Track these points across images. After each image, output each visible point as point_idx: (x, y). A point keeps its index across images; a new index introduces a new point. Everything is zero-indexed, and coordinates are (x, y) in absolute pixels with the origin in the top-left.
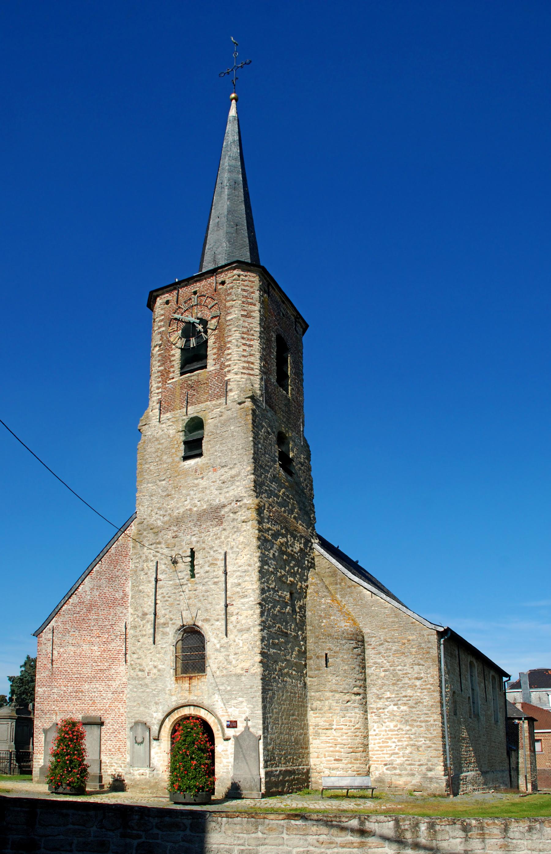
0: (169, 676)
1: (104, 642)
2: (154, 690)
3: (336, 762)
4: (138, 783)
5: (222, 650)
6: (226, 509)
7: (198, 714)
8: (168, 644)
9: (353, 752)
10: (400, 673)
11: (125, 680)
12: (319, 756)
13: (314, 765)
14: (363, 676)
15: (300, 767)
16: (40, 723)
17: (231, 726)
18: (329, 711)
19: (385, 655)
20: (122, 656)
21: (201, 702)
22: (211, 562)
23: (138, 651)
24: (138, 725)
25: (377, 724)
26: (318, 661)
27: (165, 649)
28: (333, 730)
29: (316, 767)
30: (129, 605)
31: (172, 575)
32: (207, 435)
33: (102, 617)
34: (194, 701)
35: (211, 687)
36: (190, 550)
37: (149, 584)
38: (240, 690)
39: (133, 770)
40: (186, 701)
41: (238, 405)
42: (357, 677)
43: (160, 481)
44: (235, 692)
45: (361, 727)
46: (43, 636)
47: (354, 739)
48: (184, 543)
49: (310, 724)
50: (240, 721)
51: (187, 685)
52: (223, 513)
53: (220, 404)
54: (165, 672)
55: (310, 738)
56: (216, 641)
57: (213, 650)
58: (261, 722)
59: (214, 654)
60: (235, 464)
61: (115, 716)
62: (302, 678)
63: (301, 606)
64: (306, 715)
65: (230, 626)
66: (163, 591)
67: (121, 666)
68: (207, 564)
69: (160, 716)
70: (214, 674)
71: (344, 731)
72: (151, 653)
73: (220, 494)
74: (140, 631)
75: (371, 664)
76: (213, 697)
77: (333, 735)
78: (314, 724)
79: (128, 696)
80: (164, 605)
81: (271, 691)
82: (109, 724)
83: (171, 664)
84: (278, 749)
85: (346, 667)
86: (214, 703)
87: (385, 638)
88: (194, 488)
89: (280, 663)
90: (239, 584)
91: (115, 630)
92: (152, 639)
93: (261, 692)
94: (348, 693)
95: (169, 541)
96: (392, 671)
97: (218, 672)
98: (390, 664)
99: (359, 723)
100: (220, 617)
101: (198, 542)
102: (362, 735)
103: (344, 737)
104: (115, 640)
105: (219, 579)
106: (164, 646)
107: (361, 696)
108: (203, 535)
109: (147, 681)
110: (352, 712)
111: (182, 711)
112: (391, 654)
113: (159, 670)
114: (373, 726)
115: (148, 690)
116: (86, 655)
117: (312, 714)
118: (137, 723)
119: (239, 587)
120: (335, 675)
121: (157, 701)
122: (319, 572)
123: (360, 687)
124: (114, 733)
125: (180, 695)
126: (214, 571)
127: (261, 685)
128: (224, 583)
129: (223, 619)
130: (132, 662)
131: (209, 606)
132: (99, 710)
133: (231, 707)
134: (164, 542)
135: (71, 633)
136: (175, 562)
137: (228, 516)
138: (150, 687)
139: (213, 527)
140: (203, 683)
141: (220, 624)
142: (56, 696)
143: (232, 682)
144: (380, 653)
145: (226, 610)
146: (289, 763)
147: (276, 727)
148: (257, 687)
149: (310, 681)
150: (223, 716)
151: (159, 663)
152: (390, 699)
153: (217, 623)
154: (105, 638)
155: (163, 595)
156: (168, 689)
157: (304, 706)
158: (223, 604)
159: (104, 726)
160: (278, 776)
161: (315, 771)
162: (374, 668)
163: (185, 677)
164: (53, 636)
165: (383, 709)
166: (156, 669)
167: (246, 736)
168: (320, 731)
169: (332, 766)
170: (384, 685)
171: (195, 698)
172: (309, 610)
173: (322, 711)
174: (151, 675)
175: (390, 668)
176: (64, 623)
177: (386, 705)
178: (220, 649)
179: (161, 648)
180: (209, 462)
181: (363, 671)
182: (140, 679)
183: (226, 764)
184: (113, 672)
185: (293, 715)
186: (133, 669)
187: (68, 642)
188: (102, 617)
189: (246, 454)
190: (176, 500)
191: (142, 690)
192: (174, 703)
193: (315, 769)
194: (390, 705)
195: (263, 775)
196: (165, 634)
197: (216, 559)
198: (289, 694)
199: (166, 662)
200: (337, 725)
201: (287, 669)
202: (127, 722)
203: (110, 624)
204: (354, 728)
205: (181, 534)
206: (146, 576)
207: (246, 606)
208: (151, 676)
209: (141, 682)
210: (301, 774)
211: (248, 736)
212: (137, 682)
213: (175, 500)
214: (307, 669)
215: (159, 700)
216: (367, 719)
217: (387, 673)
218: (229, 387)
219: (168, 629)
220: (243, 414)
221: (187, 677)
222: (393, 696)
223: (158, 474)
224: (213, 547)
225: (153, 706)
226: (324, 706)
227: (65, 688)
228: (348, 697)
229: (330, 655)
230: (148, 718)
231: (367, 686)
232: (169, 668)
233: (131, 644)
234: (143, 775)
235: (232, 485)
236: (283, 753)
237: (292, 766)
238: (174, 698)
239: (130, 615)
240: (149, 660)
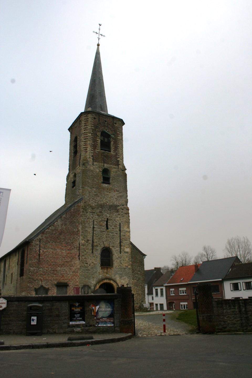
5: (119, 258)
6: (119, 207)
7: (110, 282)
10: (134, 269)
22: (115, 225)
30: (80, 235)
36: (106, 219)
40: (105, 277)
46: (34, 242)
48: (104, 215)
51: (106, 271)
56: (117, 255)
68: (113, 226)
69: (94, 282)
74: (86, 247)
79: (80, 274)
101: (110, 216)
115: (89, 272)
125: (103, 274)
126: (116, 229)
129: (119, 247)
130: (82, 260)
135: (50, 243)
137: (120, 210)
153: (117, 248)
158: (119, 241)
164: (40, 243)
171: (109, 276)
176: (46, 238)
187: (49, 247)
192: (101, 278)
196: (97, 250)
206: (89, 225)
212: (84, 268)
215: (94, 276)
219: (98, 248)
227: (47, 269)
232: (98, 263)
239: (81, 240)
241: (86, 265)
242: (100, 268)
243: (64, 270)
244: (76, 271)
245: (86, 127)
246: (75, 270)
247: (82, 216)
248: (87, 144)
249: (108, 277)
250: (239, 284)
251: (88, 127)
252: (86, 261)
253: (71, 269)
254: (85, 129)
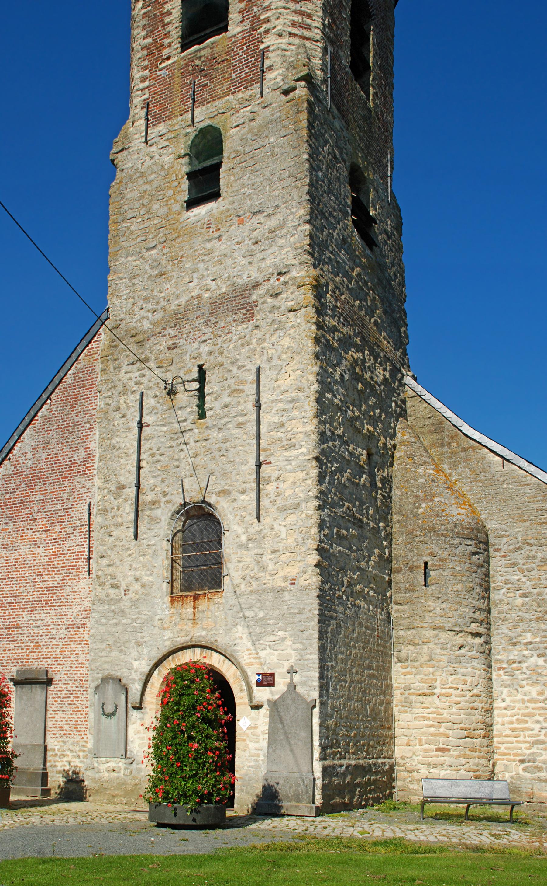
0: (159, 595)
1: (54, 539)
2: (135, 620)
3: (439, 753)
4: (105, 785)
7: (207, 661)
8: (159, 539)
9: (468, 737)
11: (87, 604)
12: (411, 743)
13: (401, 757)
14: (486, 604)
15: (380, 761)
17: (264, 682)
18: (429, 663)
19: (525, 567)
20: (82, 563)
21: (213, 640)
23: (109, 552)
24: (108, 683)
25: (508, 689)
26: (411, 575)
27: (154, 547)
28: (435, 697)
29: (404, 762)
31: (166, 416)
32: (228, 157)
33: (51, 496)
34: (201, 639)
35: (230, 613)
37: (128, 434)
38: (280, 616)
39: (97, 762)
40: (188, 638)
41: (283, 97)
42: (477, 604)
43: (148, 249)
44: (271, 621)
45: (482, 693)
47: (470, 714)
49: (395, 685)
50: (279, 674)
51: (191, 610)
52: (254, 297)
53: (251, 98)
54: (154, 587)
55: (396, 709)
57: (235, 545)
58: (317, 675)
59: (237, 553)
60: (277, 207)
61: (71, 667)
62: (385, 604)
63: (385, 478)
64: (389, 669)
65: (264, 502)
66: (152, 445)
67: (81, 580)
70: (236, 589)
71: (453, 698)
72: (130, 555)
73: (250, 263)
74: (113, 517)
75: (499, 584)
76: (234, 630)
77: (434, 705)
78: (403, 686)
80: (153, 469)
81: (334, 621)
82: (60, 682)
83: (163, 574)
84: (344, 727)
85: (459, 587)
86: (236, 642)
87: (525, 537)
88: (205, 257)
89: (349, 572)
90: (282, 425)
91: (71, 518)
92: (132, 530)
93: (316, 620)
94: (461, 631)
95: (161, 356)
96: (535, 596)
97: (243, 586)
98: (533, 583)
99: (479, 686)
100: (248, 486)
102: (482, 708)
103: (454, 710)
104: (72, 535)
105: (246, 417)
106: (153, 542)
107: (482, 638)
108: (220, 340)
109: (125, 604)
110: (468, 665)
111: (180, 657)
112: (534, 565)
113: (143, 586)
114: (502, 693)
116: (26, 563)
117: (400, 669)
118: (105, 680)
119: (282, 430)
120: (440, 600)
121: (139, 639)
122: (412, 425)
123: (481, 622)
124: (69, 697)
125: (177, 628)
127: (317, 607)
128: (255, 423)
130: (100, 573)
131: (229, 467)
132: (44, 658)
133: (265, 649)
134: (153, 358)
136: (172, 392)
138: (128, 616)
139: (237, 325)
140: (217, 606)
141: (248, 498)
143: (268, 604)
144: (515, 565)
145: (258, 473)
146: (362, 753)
147: (341, 686)
148: (310, 611)
149: (397, 611)
150: (251, 664)
151: (143, 573)
152: (532, 646)
154: (56, 532)
155: (151, 452)
156: (157, 617)
157: (386, 654)
159: (53, 686)
160: (344, 774)
161: (404, 768)
162: (504, 590)
163: (187, 596)
165: (520, 662)
166: (139, 584)
167: (289, 702)
168: (413, 698)
169: (432, 760)
170: (521, 620)
171: (204, 633)
172: (397, 488)
173: (417, 663)
174: (131, 595)
175: (532, 590)
177: (524, 656)
178: (247, 545)
179: (148, 545)
180: (231, 207)
181: (487, 595)
182: (112, 603)
183: (253, 752)
184: (68, 591)
185: (369, 668)
186: (100, 585)
188: (51, 496)
189: (296, 187)
190: (175, 282)
191: (115, 621)
192: (168, 643)
193: (404, 766)
194: (532, 656)
195: (318, 774)
197: (242, 382)
198: (364, 629)
199: (155, 570)
200: (442, 688)
201: (361, 586)
202: (90, 679)
203: (65, 507)
204: (471, 694)
205: (182, 342)
207: (294, 463)
208: (130, 596)
209: (113, 607)
210: (381, 773)
211: (294, 701)
212: (107, 607)
213: (173, 281)
214: (393, 590)
216: (491, 680)
217: (527, 599)
218: (267, 63)
220: (291, 112)
221: (191, 596)
222: (538, 640)
223: (144, 238)
224: (237, 360)
225: (134, 648)
226: (420, 654)
228: (461, 639)
229: (433, 565)
230: (125, 670)
231: (492, 623)
232: (160, 581)
233: (97, 540)
234: (114, 771)
235: (272, 246)
236: (352, 735)
237: (365, 758)
238: (168, 634)
240: (127, 567)
241: (112, 591)
243: (39, 623)
244: (78, 622)
246: (75, 618)
249: (201, 636)
252: (113, 577)
253: (61, 616)
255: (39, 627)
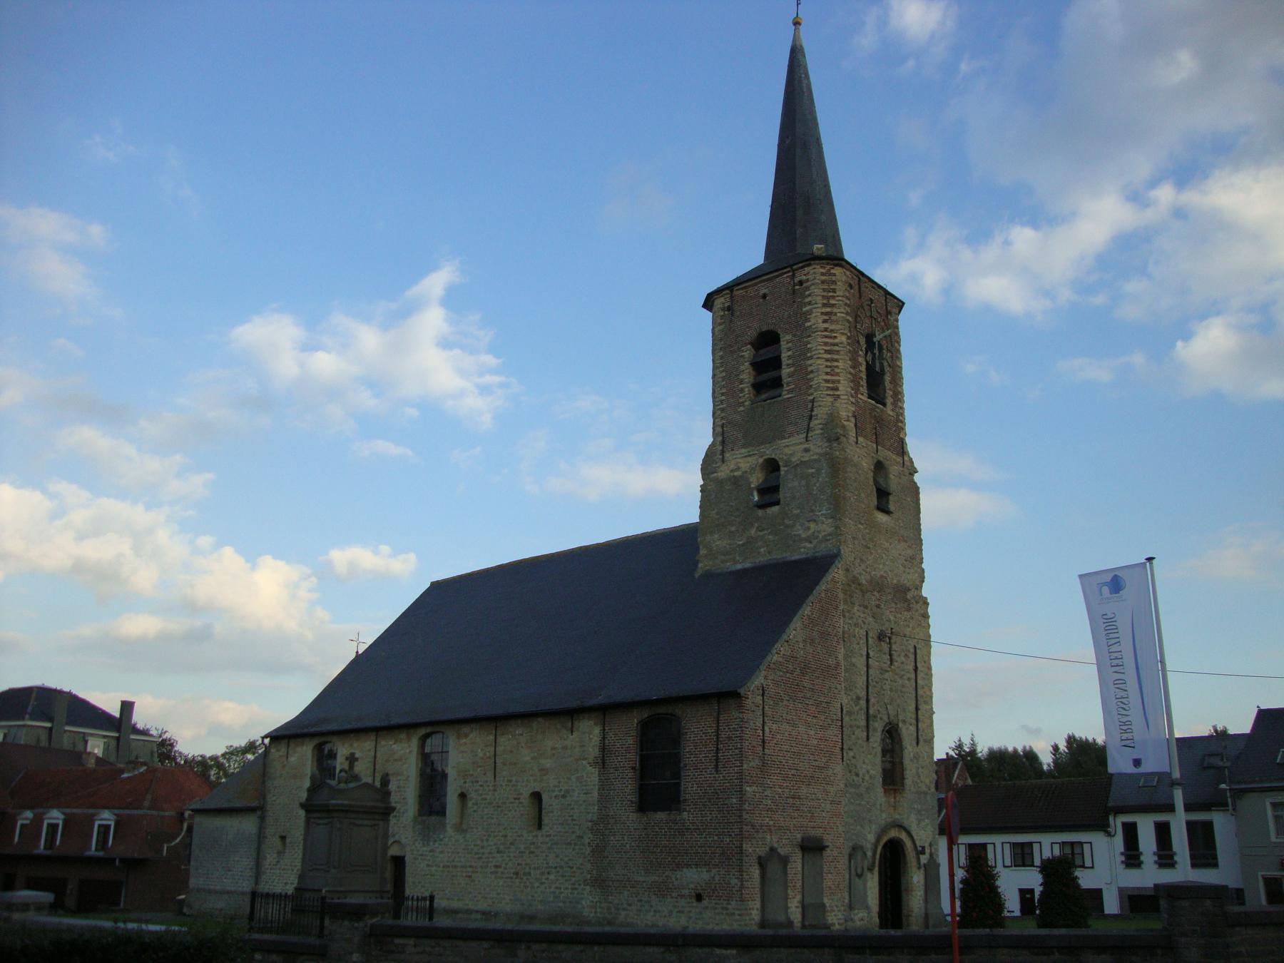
16: (750, 847)
20: (838, 751)
30: (842, 679)
113: (871, 777)
142: (770, 802)
192: (883, 822)
221: (891, 789)
227: (780, 790)
238: (884, 816)
241: (855, 778)
242: (882, 790)
245: (828, 310)
247: (844, 616)
248: (837, 370)
250: (990, 848)
251: (835, 310)
254: (826, 318)
255: (813, 800)
